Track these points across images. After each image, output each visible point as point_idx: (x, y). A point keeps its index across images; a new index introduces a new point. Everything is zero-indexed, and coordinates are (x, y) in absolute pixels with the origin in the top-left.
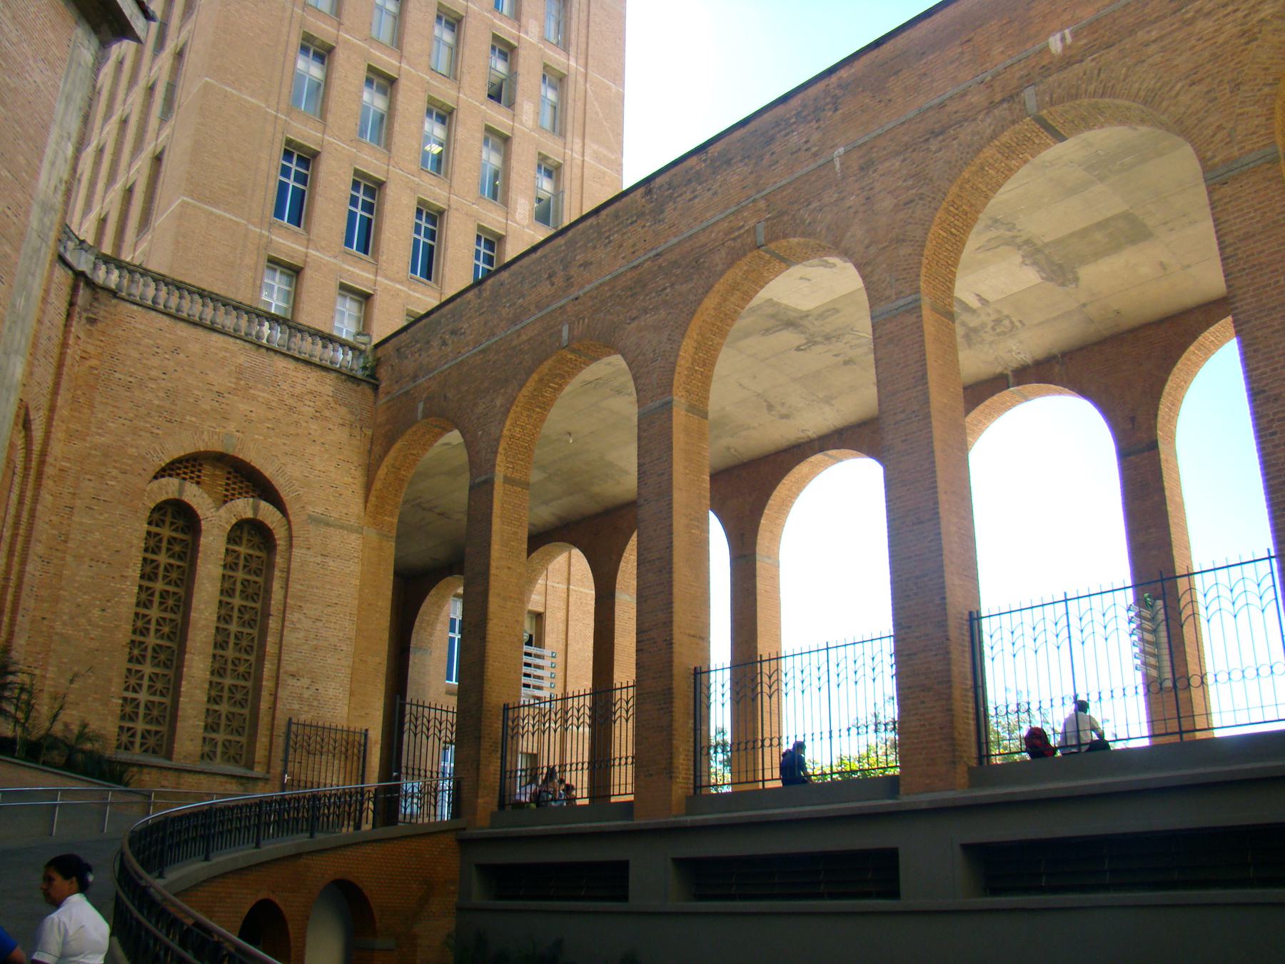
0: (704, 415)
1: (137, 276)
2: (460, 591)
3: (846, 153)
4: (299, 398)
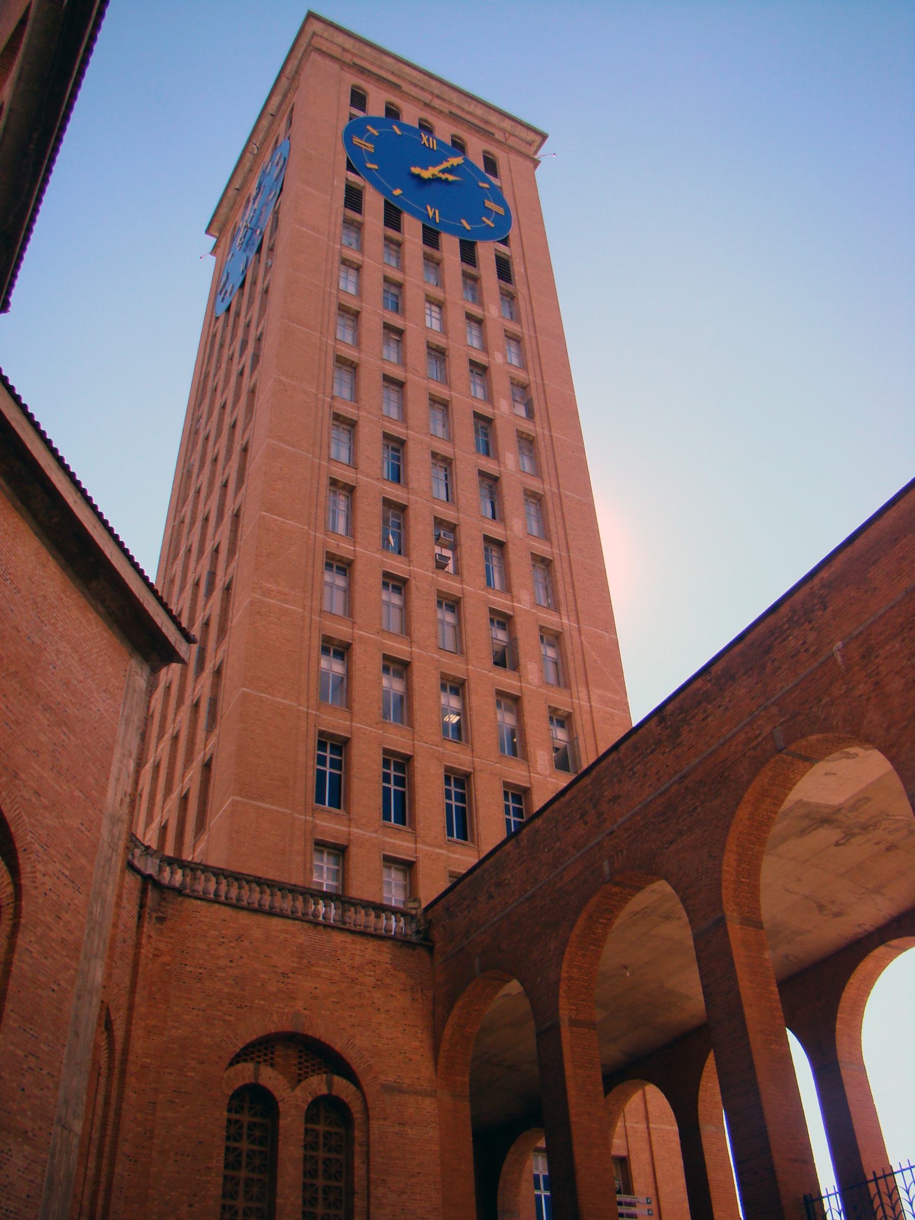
0: (759, 925)
1: (199, 873)
2: (542, 1144)
3: (845, 646)
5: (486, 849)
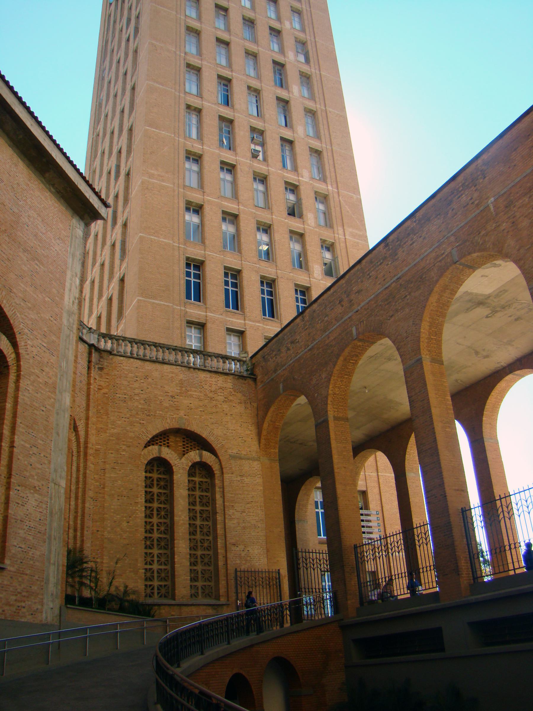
0: (441, 363)
1: (121, 341)
2: (319, 485)
3: (495, 200)
4: (215, 392)
5: (285, 323)
